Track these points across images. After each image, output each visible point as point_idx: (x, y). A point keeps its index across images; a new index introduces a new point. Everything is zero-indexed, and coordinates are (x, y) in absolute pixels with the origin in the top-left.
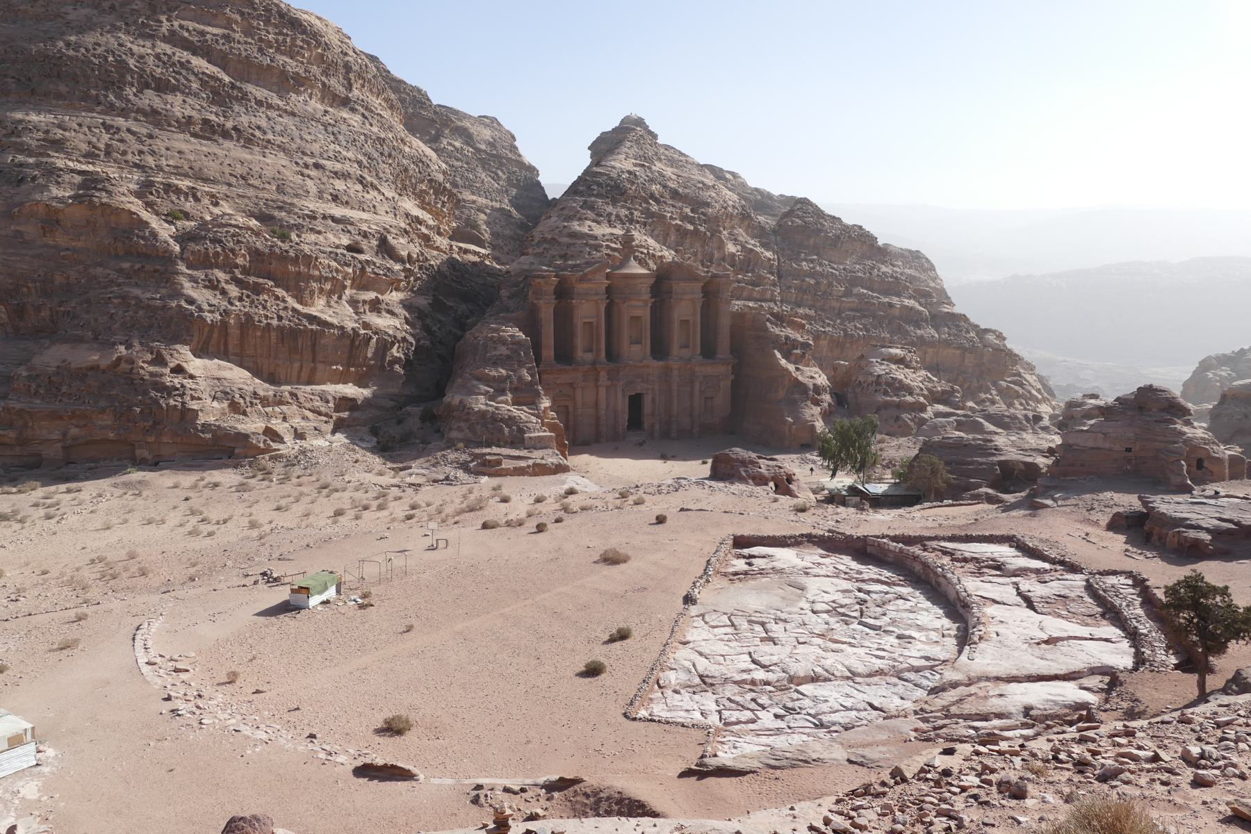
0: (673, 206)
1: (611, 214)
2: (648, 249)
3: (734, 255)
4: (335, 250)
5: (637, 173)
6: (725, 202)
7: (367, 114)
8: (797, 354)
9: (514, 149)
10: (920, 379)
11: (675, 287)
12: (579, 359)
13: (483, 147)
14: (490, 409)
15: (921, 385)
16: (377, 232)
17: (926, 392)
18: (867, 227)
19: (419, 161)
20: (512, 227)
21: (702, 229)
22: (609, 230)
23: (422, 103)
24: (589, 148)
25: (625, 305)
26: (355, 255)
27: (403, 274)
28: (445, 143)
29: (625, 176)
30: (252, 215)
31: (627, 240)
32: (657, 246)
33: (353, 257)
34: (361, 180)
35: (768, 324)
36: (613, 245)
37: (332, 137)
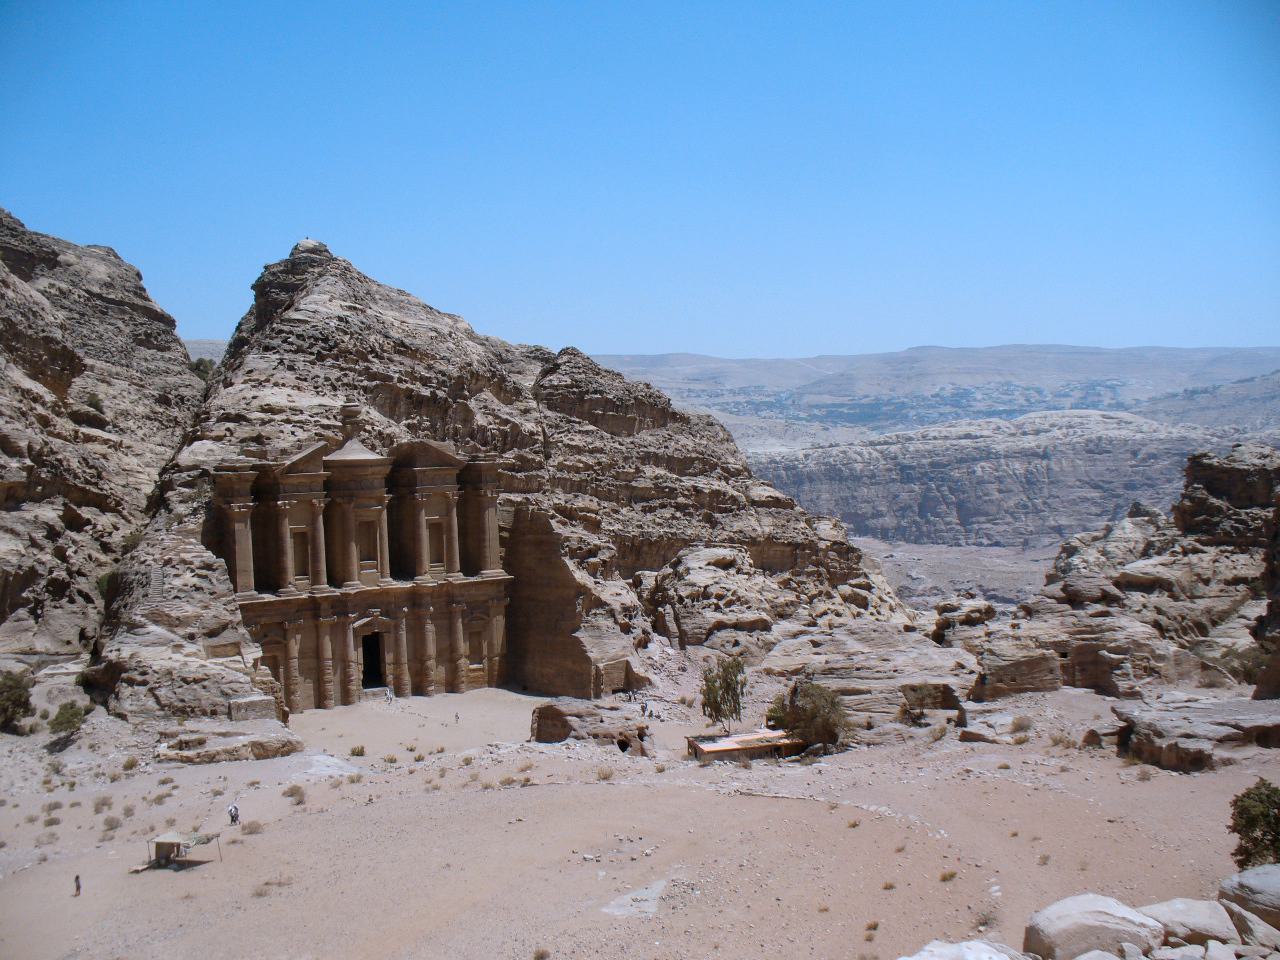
1: (318, 377)
2: (372, 424)
5: (350, 319)
9: (140, 291)
10: (757, 588)
13: (96, 289)
14: (177, 665)
15: (760, 597)
17: (767, 606)
19: (31, 313)
20: (147, 402)
21: (440, 394)
24: (253, 287)
25: (352, 505)
27: (25, 474)
28: (46, 285)
29: (334, 323)
31: (348, 415)
32: (385, 419)
35: (553, 522)
36: (325, 422)
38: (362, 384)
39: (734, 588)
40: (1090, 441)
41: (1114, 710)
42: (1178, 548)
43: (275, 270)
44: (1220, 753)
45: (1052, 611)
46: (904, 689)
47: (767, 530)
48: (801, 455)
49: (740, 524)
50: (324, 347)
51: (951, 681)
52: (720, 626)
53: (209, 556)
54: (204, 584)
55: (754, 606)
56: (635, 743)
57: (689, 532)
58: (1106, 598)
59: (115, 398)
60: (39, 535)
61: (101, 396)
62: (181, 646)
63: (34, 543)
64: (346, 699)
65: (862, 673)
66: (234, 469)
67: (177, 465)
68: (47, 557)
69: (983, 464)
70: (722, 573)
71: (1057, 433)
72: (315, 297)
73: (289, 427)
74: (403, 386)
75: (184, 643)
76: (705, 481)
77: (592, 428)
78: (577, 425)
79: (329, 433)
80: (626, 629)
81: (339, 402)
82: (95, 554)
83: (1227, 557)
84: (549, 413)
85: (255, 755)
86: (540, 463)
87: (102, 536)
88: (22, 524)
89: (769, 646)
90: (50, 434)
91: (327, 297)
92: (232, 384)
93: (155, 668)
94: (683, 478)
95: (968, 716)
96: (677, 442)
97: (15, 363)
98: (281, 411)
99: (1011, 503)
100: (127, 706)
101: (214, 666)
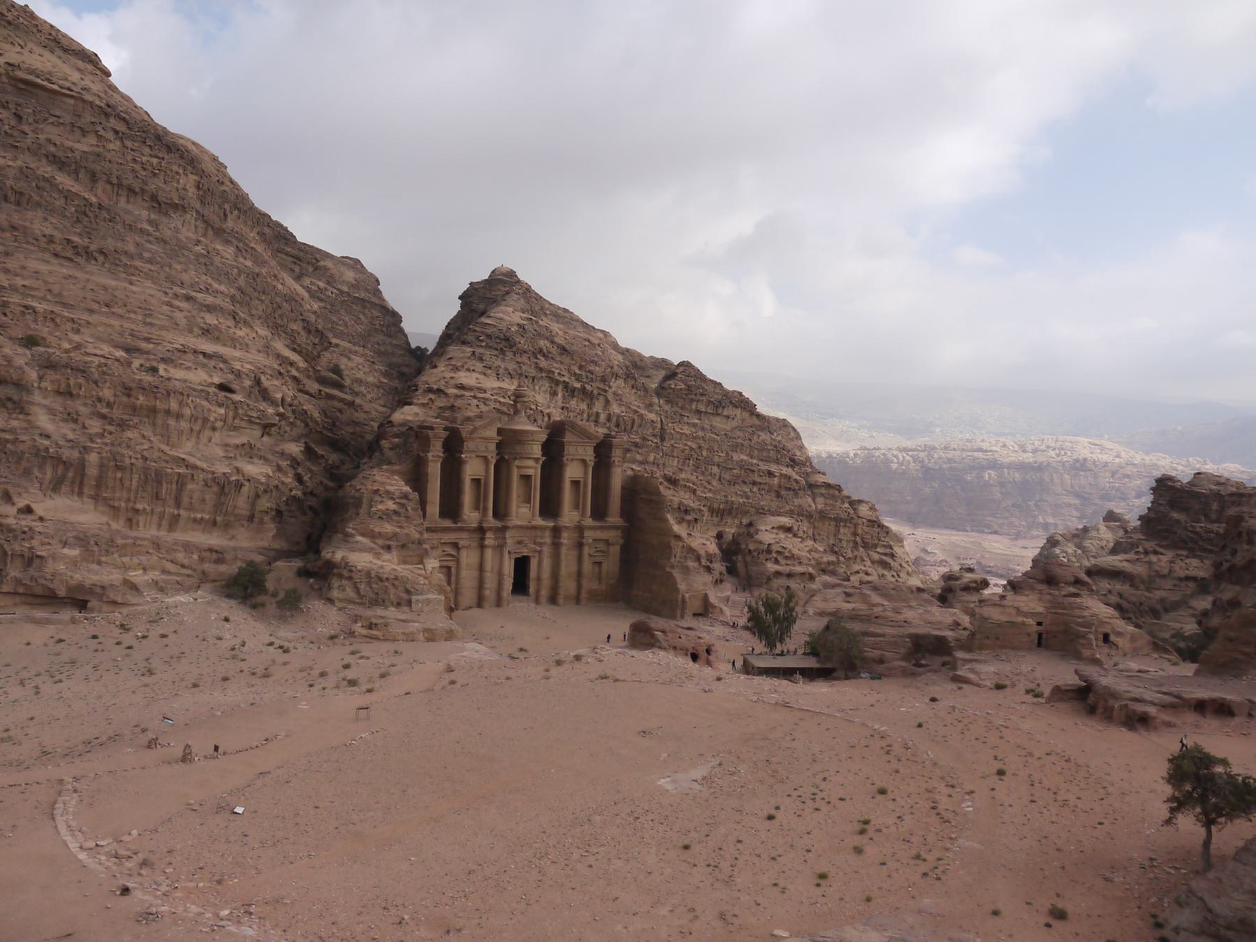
0: (562, 363)
1: (500, 367)
2: (537, 405)
3: (619, 416)
4: (207, 388)
5: (526, 327)
6: (610, 360)
7: (241, 245)
8: (689, 522)
9: (377, 293)
10: (807, 549)
11: (566, 447)
12: (465, 517)
13: (345, 289)
16: (251, 371)
17: (813, 562)
18: (746, 394)
19: (291, 298)
20: (376, 375)
21: (588, 387)
22: (497, 384)
23: (286, 239)
24: (460, 298)
26: (228, 394)
30: (117, 346)
33: (226, 397)
34: (234, 316)
35: (661, 488)
36: (502, 400)
37: (203, 267)
38: (531, 375)
39: (790, 547)
40: (1077, 461)
41: (1076, 672)
42: (1140, 549)
43: (477, 286)
44: (1165, 717)
45: (1032, 588)
46: (911, 636)
47: (819, 507)
48: (852, 455)
49: (800, 500)
50: (505, 343)
51: (948, 634)
52: (778, 574)
53: (407, 489)
54: (401, 511)
55: (805, 561)
56: (704, 655)
57: (762, 503)
58: (1077, 582)
59: (352, 369)
60: (284, 464)
61: (342, 367)
62: (379, 553)
63: (279, 468)
64: (499, 602)
65: (880, 621)
66: (432, 428)
67: (391, 422)
68: (289, 480)
69: (990, 471)
70: (782, 535)
71: (1052, 453)
72: (502, 308)
73: (475, 402)
74: (562, 379)
75: (382, 551)
76: (776, 467)
77: (697, 421)
78: (686, 418)
79: (505, 409)
80: (709, 569)
81: (510, 386)
82: (325, 481)
83: (1181, 560)
84: (667, 407)
85: (425, 638)
86: (657, 443)
87: (332, 468)
88: (273, 454)
89: (813, 594)
90: (300, 391)
91: (512, 309)
92: (435, 367)
93: (359, 568)
94: (760, 463)
95: (959, 663)
96: (759, 436)
97: (279, 336)
98: (470, 389)
99: (1009, 503)
100: (335, 594)
101: (403, 570)
